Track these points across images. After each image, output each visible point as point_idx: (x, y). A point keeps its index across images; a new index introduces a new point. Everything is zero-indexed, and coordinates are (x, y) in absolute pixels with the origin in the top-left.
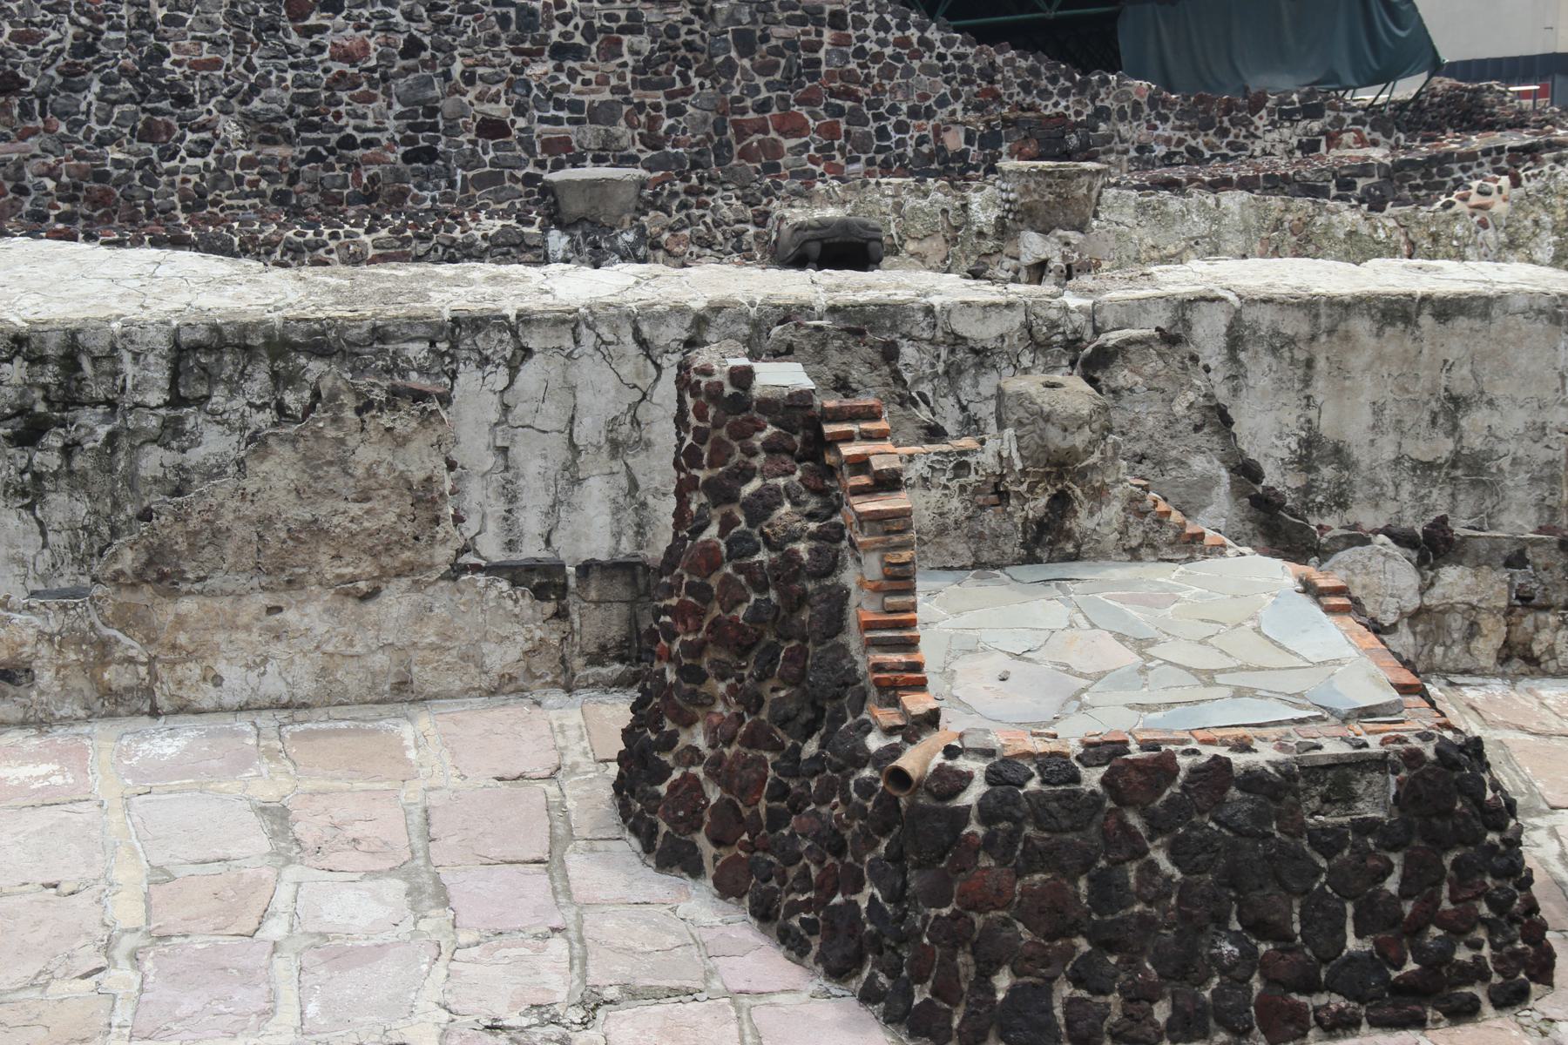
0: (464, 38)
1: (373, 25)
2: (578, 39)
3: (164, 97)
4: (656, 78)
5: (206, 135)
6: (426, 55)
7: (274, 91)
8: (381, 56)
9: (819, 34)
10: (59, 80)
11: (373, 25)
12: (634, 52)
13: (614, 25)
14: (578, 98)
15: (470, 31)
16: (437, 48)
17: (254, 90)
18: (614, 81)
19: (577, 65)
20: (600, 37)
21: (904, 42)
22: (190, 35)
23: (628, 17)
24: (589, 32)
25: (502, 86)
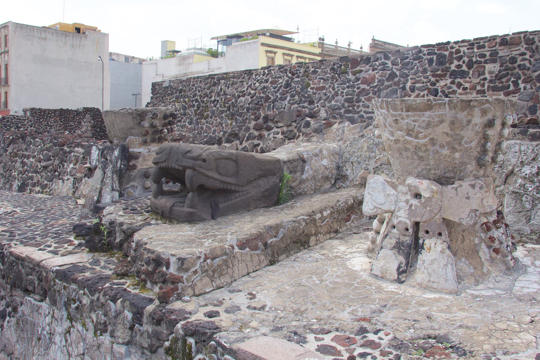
0: (413, 71)
1: (379, 68)
2: (464, 68)
3: (305, 102)
4: (500, 85)
6: (396, 79)
7: (340, 97)
8: (379, 81)
10: (279, 96)
11: (379, 68)
12: (490, 73)
13: (483, 60)
15: (415, 67)
16: (401, 76)
18: (479, 88)
19: (461, 81)
20: (475, 66)
22: (318, 77)
23: (490, 55)
24: (470, 65)
25: (426, 92)
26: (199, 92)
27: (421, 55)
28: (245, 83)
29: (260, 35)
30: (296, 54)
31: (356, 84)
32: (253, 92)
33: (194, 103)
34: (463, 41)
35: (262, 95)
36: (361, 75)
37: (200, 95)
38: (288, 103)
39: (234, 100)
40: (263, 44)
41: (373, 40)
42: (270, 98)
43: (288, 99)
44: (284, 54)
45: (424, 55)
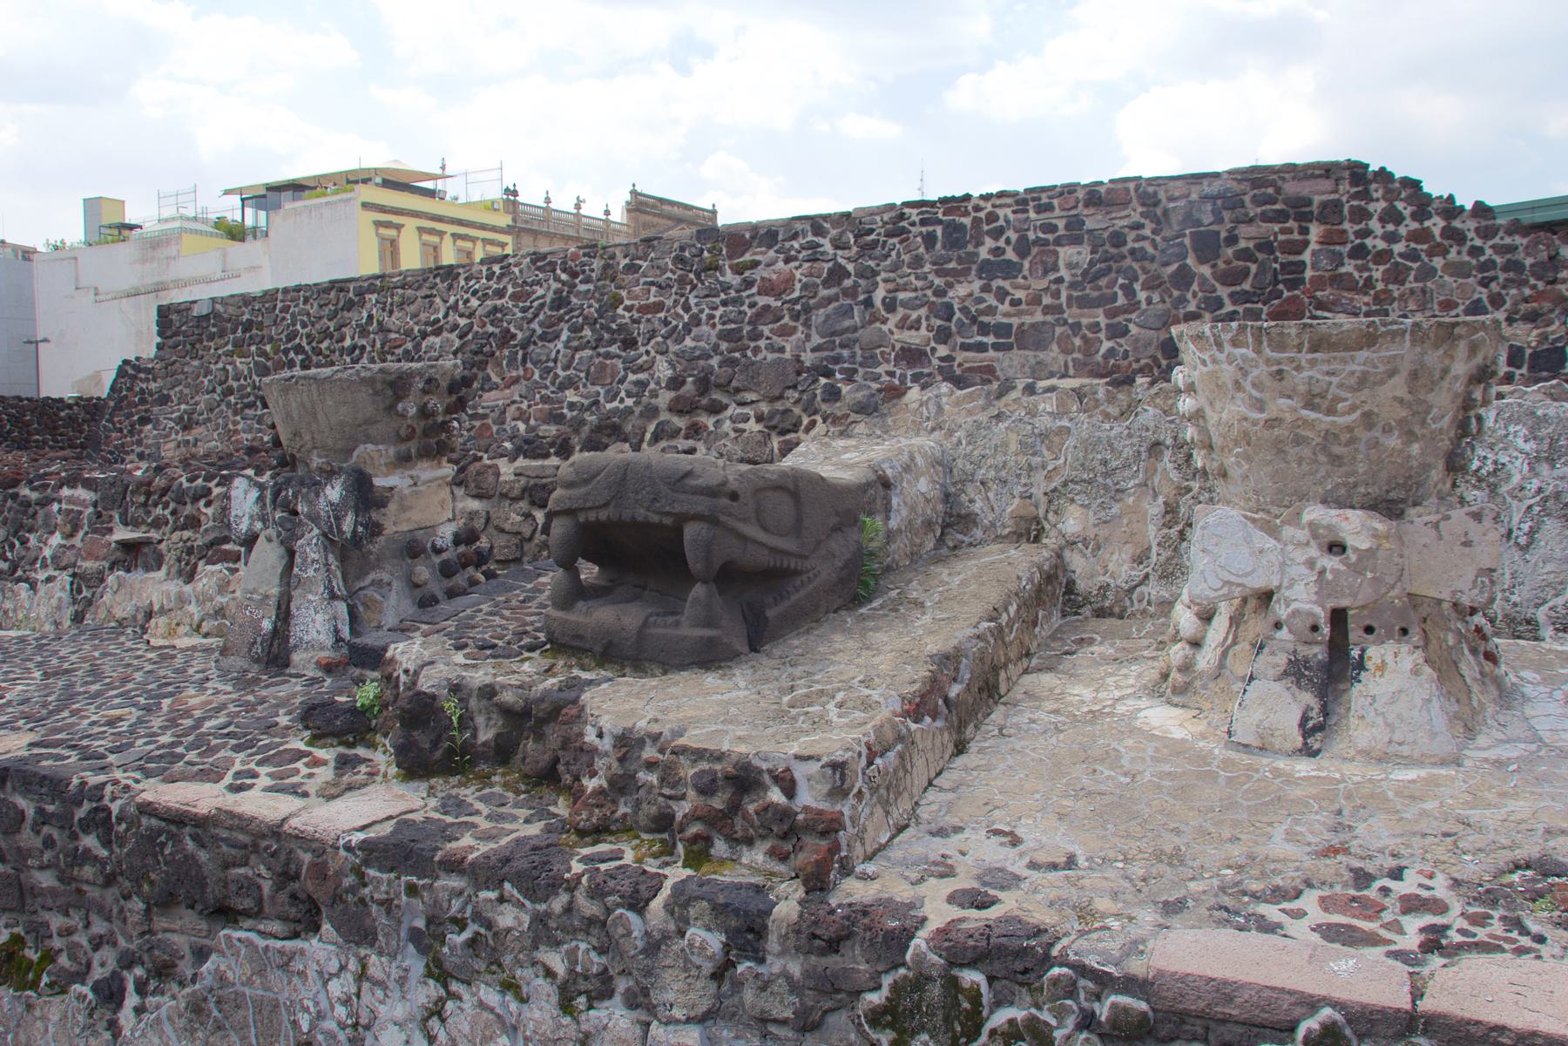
0: (888, 262)
1: (801, 256)
2: (1010, 255)
3: (611, 342)
4: (1095, 294)
5: (642, 376)
6: (847, 283)
7: (705, 328)
8: (805, 287)
9: (1304, 231)
10: (539, 331)
11: (801, 256)
12: (1071, 266)
13: (1050, 237)
14: (1005, 320)
15: (894, 254)
16: (860, 275)
17: (688, 329)
18: (1047, 300)
19: (1006, 284)
20: (1035, 250)
21: (1422, 236)
22: (642, 280)
23: (1067, 227)
24: (1023, 248)
25: (923, 312)
26: (304, 326)
27: (904, 224)
28: (438, 300)
29: (356, 182)
30: (450, 229)
31: (744, 294)
32: (463, 322)
33: (292, 355)
34: (1002, 194)
35: (490, 329)
36: (758, 274)
37: (308, 336)
38: (566, 347)
39: (409, 346)
40: (366, 206)
41: (634, 193)
42: (514, 336)
43: (564, 337)
44: (421, 230)
45: (913, 224)
